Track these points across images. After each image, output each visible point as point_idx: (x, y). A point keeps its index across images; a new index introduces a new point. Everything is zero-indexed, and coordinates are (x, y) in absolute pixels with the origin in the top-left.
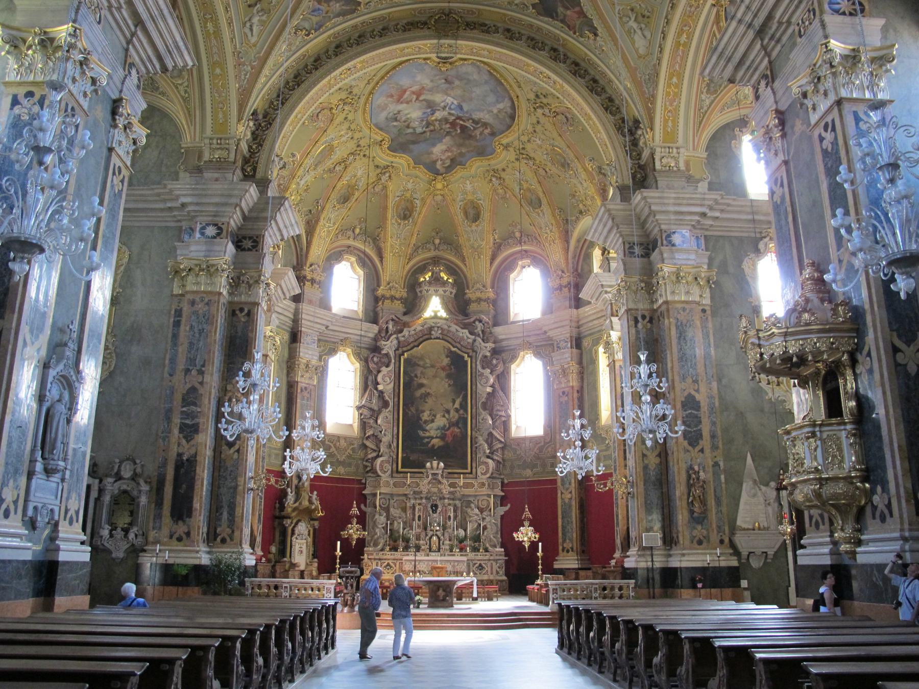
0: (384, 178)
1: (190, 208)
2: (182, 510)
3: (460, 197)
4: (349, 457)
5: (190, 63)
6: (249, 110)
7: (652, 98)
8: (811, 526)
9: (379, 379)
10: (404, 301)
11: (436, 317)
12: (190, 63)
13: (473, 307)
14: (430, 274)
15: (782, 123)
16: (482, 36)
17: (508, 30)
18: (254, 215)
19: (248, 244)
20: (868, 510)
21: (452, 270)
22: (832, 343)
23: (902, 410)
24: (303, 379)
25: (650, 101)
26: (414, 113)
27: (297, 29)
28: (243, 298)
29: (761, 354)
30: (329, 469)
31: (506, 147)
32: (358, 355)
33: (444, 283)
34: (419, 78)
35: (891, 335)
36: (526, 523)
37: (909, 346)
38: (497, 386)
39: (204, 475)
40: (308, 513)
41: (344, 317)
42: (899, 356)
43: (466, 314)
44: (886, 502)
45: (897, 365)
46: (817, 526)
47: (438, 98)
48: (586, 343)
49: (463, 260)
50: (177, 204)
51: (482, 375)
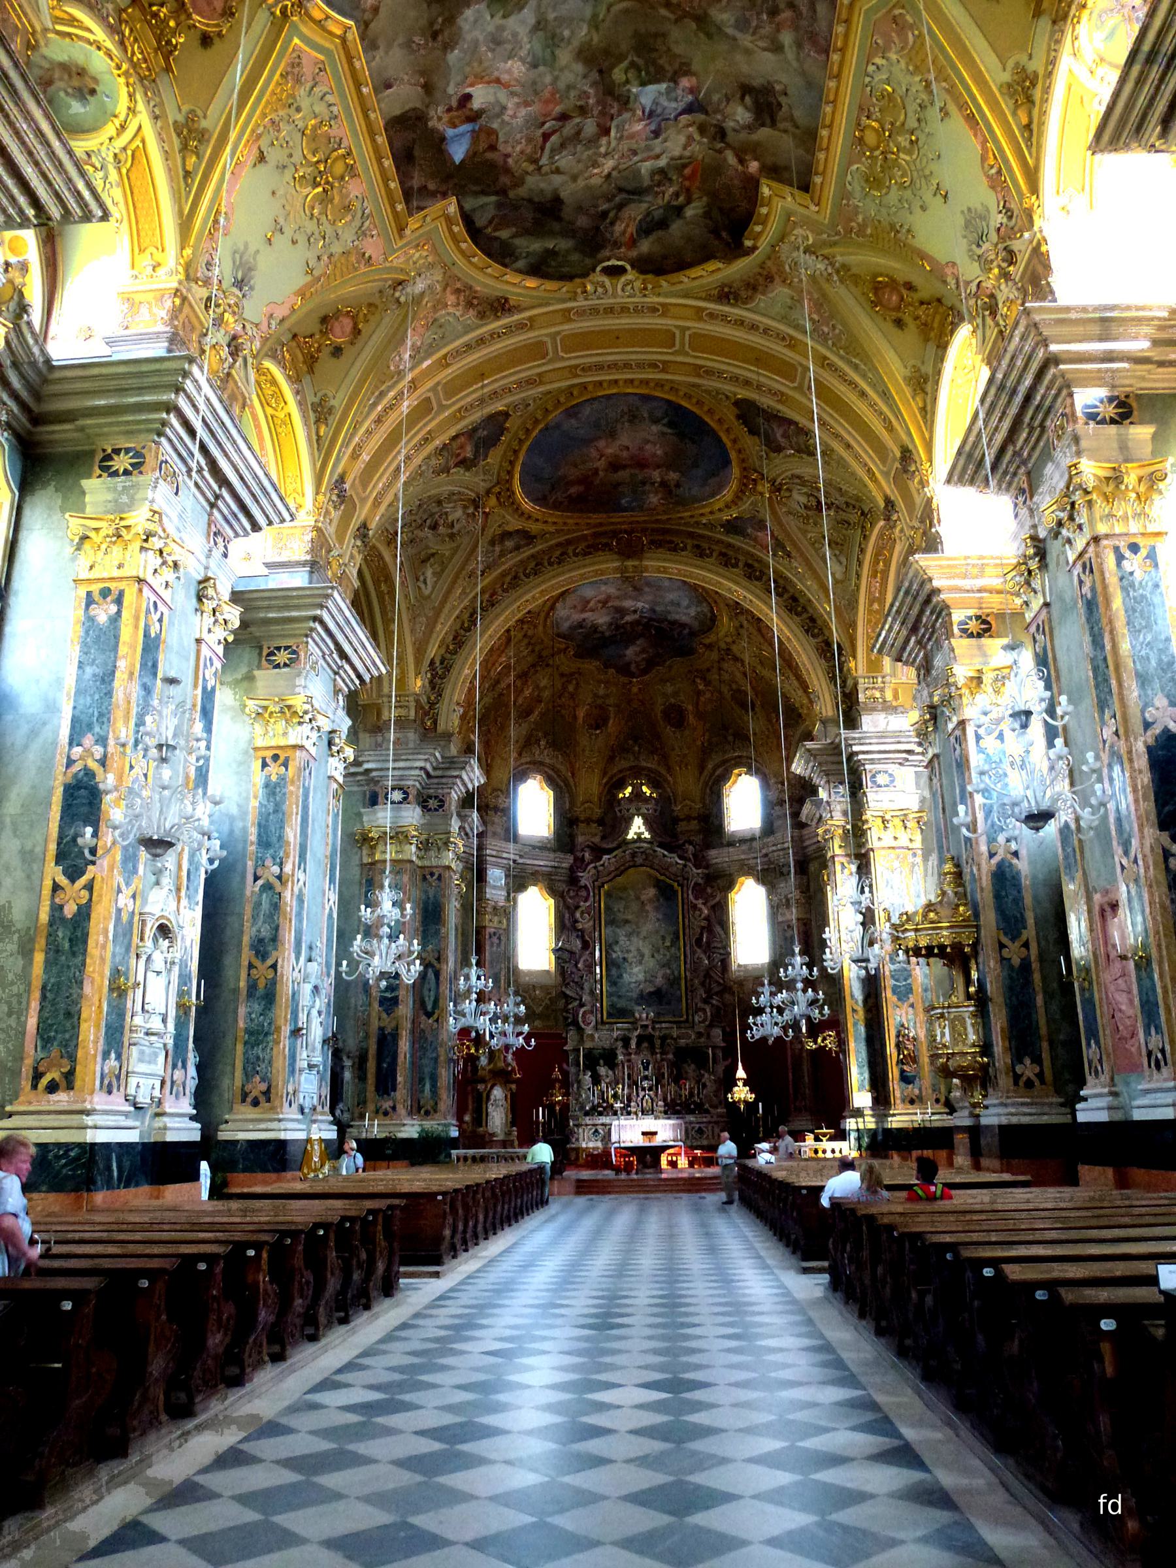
0: (571, 688)
1: (374, 774)
2: (386, 1084)
3: (660, 700)
4: (547, 1007)
5: (384, 671)
6: (427, 663)
7: (853, 625)
9: (578, 915)
10: (601, 822)
11: (639, 839)
12: (384, 671)
13: (682, 826)
14: (629, 789)
15: (934, 718)
16: (668, 555)
17: (698, 547)
18: (439, 773)
19: (432, 803)
21: (655, 784)
24: (492, 923)
25: (849, 626)
26: (602, 619)
27: (472, 575)
28: (434, 862)
30: (533, 1042)
31: (709, 647)
32: (552, 891)
33: (647, 800)
34: (603, 588)
36: (740, 1083)
38: (713, 920)
39: (404, 1046)
40: (501, 1076)
41: (534, 847)
42: (1005, 952)
43: (675, 836)
45: (1003, 959)
47: (628, 604)
48: (813, 867)
49: (669, 769)
50: (360, 770)
51: (695, 907)
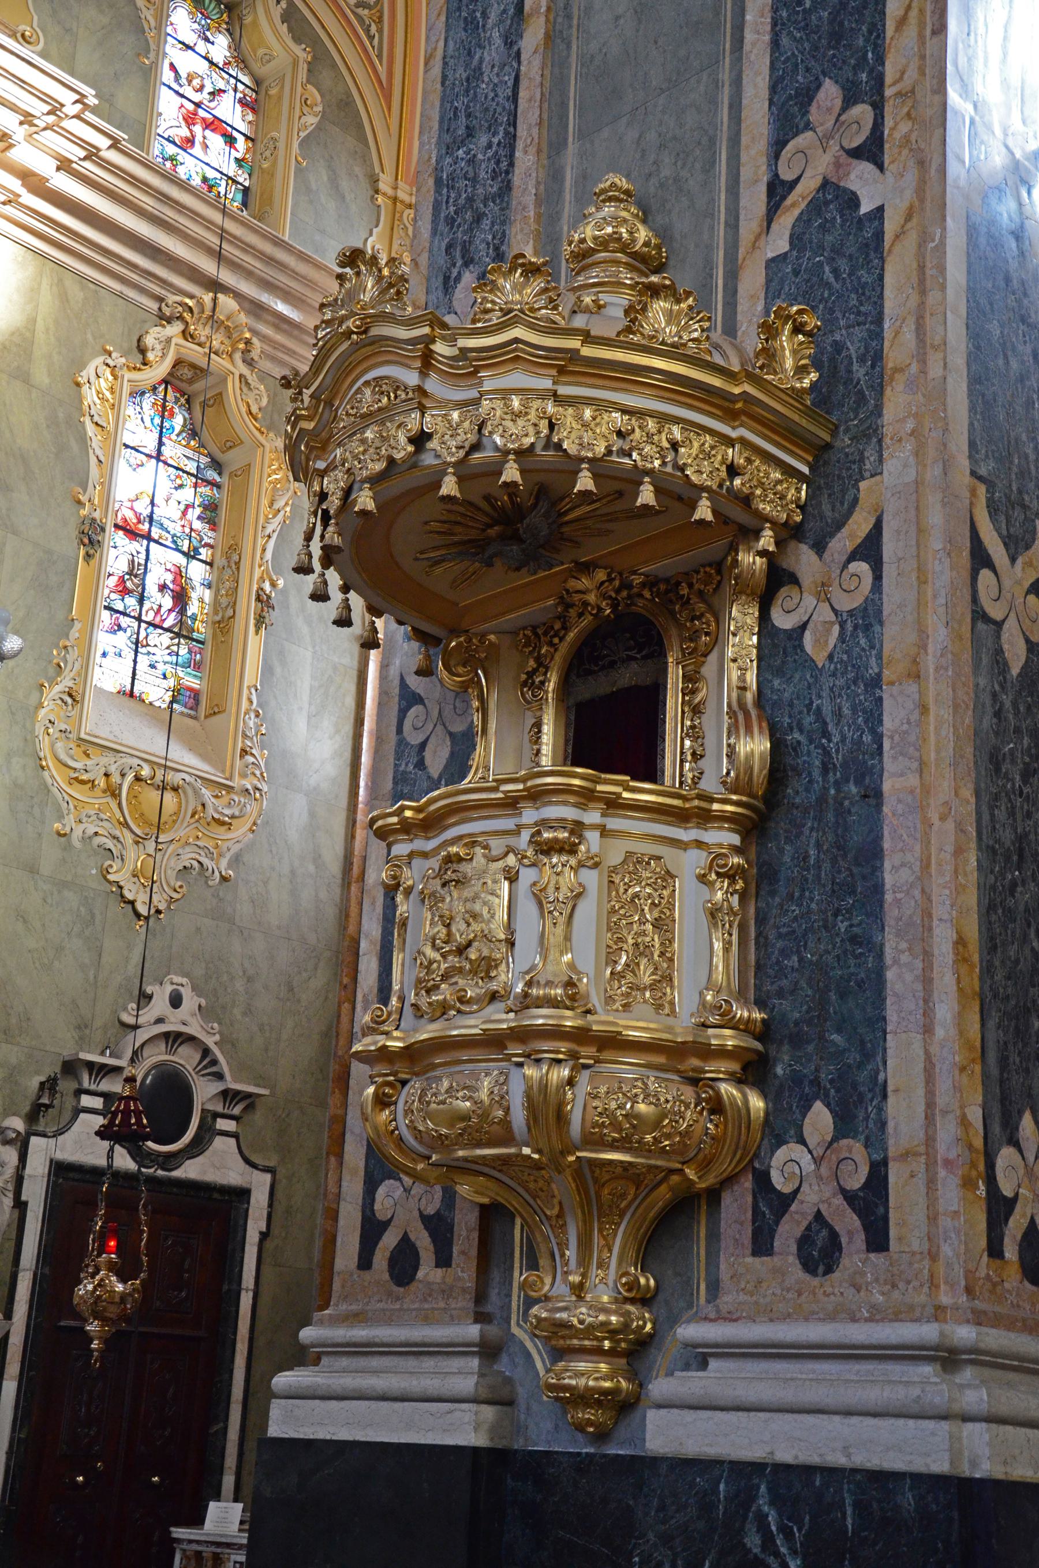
8: (365, 1262)
20: (737, 1207)
22: (733, 471)
23: (977, 794)
29: (420, 440)
35: (973, 492)
37: (1013, 560)
44: (856, 1181)
46: (404, 1266)
